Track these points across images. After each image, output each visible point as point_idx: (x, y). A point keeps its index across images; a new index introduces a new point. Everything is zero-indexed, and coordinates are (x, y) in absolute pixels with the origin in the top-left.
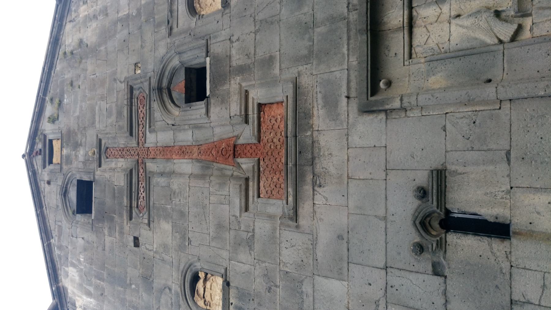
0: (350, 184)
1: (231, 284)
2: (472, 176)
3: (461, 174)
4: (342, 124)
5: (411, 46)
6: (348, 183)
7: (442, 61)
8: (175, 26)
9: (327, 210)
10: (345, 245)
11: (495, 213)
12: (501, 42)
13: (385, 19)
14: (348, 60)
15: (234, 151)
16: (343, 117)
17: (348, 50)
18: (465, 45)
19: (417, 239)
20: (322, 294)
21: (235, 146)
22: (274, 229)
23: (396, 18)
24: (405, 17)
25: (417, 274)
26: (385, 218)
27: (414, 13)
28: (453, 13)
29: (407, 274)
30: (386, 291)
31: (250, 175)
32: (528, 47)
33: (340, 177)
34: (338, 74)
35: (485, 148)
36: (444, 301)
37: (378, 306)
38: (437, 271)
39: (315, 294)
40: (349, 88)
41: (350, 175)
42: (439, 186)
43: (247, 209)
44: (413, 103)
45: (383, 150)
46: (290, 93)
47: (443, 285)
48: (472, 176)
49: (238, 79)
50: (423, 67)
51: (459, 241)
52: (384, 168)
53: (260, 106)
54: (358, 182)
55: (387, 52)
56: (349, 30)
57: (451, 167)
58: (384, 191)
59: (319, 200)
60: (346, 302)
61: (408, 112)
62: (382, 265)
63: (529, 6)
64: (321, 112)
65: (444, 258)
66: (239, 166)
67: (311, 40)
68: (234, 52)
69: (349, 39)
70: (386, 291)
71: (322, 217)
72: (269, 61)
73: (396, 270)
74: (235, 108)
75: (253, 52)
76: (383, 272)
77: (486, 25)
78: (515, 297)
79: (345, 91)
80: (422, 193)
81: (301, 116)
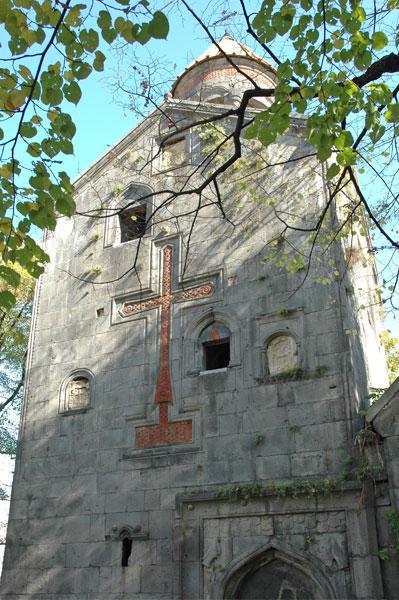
1: (85, 415)
8: (261, 322)
9: (130, 479)
15: (164, 400)
16: (176, 484)
21: (166, 402)
22: (117, 444)
31: (148, 419)
33: (145, 485)
38: (107, 537)
43: (128, 420)
46: (195, 446)
49: (207, 402)
53: (189, 422)
59: (134, 474)
64: (180, 471)
66: (154, 408)
67: (222, 459)
68: (226, 395)
69: (218, 484)
72: (215, 428)
74: (189, 402)
75: (222, 413)
80: (138, 530)
81: (178, 458)
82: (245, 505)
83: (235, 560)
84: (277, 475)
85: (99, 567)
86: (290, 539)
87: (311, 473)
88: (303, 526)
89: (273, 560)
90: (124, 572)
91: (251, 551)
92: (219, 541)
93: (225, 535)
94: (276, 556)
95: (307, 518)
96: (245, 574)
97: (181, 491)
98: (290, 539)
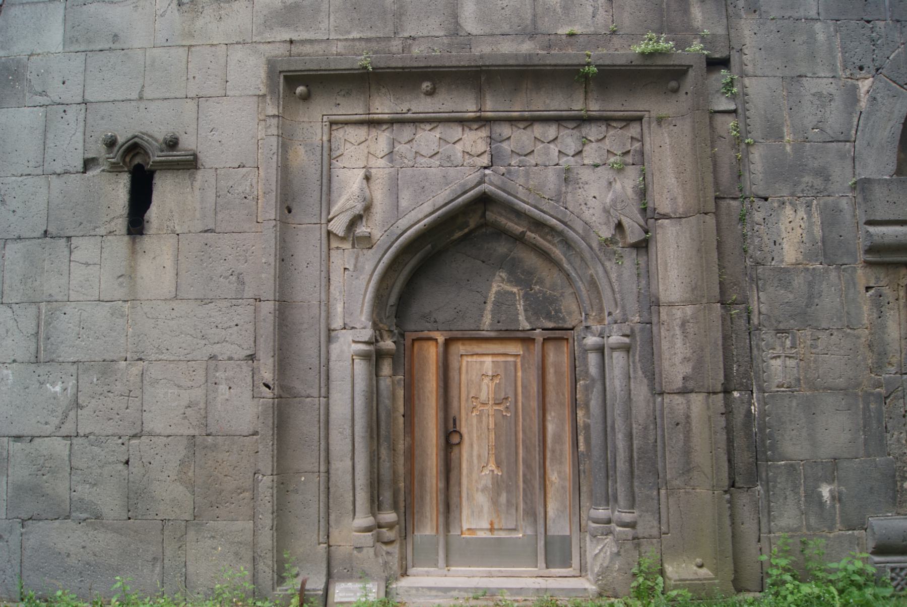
0: (181, 50)
2: (190, 197)
3: (192, 184)
4: (260, 33)
5: (347, 123)
6: (184, 46)
7: (320, 162)
10: (107, 47)
11: (152, 220)
12: (329, 221)
13: (383, 90)
14: (340, 40)
16: (268, 36)
17: (353, 40)
18: (335, 185)
19: (121, 140)
20: (44, 15)
23: (382, 104)
24: (380, 116)
25: (82, 141)
26: (141, 98)
27: (385, 127)
28: (373, 171)
29: (81, 129)
30: (59, 104)
32: (318, 245)
34: (323, 26)
35: (218, 209)
36: (58, 171)
37: (41, 95)
38: (88, 164)
39: (42, 5)
40: (303, 42)
41: (193, 49)
42: (178, 163)
44: (269, 130)
45: (222, 92)
47: (75, 170)
48: (190, 197)
50: (317, 140)
51: (122, 185)
52: (200, 95)
54: (184, 61)
55: (343, 93)
56: (378, 39)
57: (200, 175)
58: (173, 95)
60: (39, 51)
61: (263, 123)
62: (88, 97)
63: (361, 246)
65: (103, 171)
69: (368, 40)
70: (59, 104)
71: (140, 9)
73: (83, 115)
76: (80, 100)
77: (348, 207)
78: (73, 240)
79: (301, 38)
80: (172, 144)
82: (431, 93)
83: (403, 223)
84: (506, 28)
85: (69, 238)
86: (527, 174)
87: (577, 29)
88: (554, 149)
89: (479, 227)
90: (134, 252)
91: (440, 199)
92: (367, 178)
93: (382, 162)
94: (491, 216)
95: (564, 132)
96: (418, 256)
97: (280, 50)
98: (527, 174)
